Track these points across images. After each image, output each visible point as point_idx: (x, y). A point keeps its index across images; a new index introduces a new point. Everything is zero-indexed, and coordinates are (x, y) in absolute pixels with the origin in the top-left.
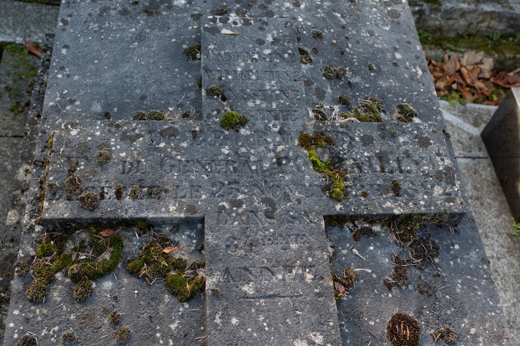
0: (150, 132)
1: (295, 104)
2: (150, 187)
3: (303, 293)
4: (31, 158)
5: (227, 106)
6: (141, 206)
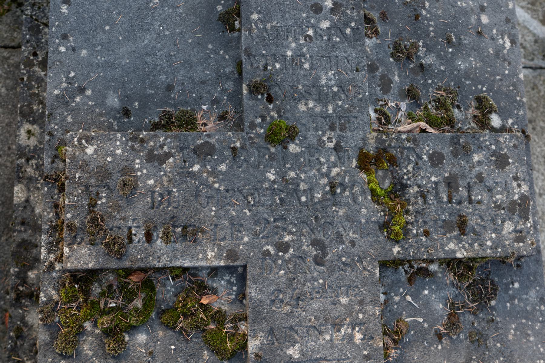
0: (181, 149)
1: (355, 108)
2: (185, 227)
3: (351, 355)
4: (32, 115)
5: (273, 111)
6: (176, 251)
